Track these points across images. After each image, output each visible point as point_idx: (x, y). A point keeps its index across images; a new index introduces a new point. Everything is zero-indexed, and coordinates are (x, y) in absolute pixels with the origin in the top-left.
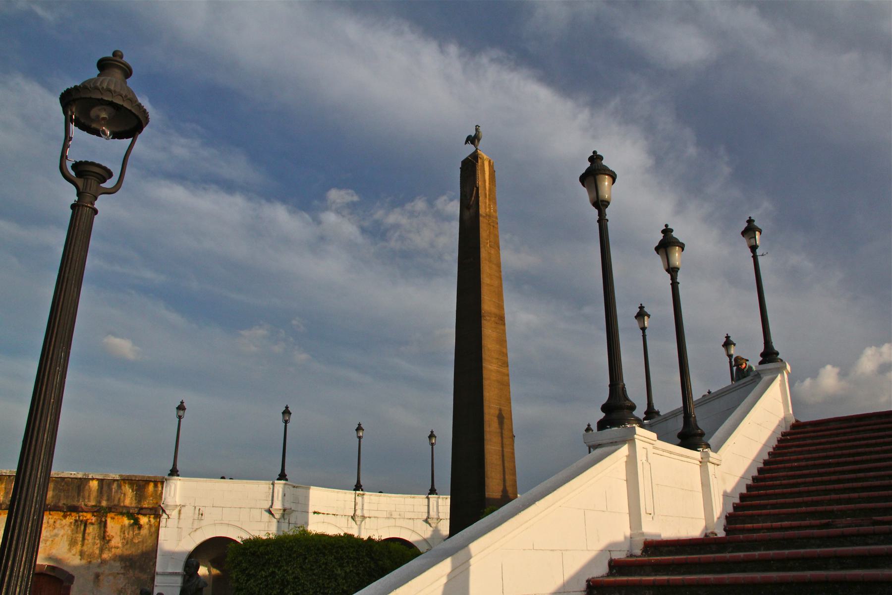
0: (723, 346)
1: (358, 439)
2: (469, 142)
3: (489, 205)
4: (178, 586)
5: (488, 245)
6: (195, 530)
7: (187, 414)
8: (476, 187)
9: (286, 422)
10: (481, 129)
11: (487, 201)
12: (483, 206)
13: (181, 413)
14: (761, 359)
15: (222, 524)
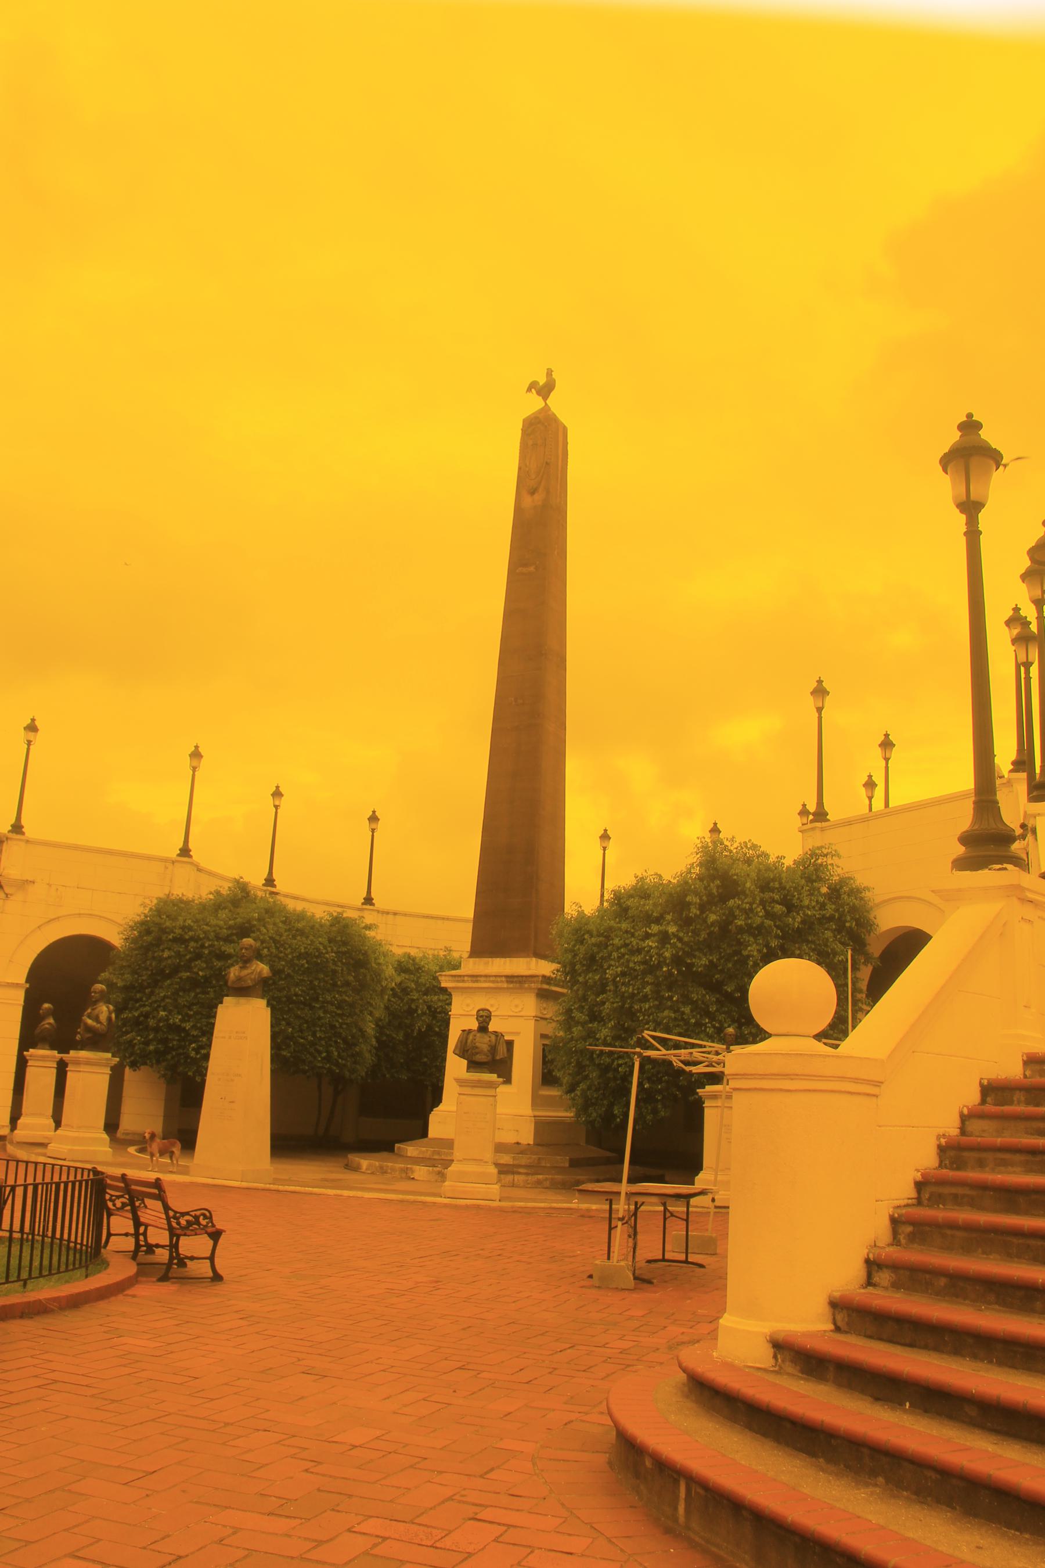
0: (880, 745)
2: (533, 390)
4: (19, 1005)
5: (556, 553)
6: (49, 921)
7: (39, 739)
8: (547, 463)
10: (554, 376)
11: (559, 487)
13: (31, 736)
15: (90, 915)
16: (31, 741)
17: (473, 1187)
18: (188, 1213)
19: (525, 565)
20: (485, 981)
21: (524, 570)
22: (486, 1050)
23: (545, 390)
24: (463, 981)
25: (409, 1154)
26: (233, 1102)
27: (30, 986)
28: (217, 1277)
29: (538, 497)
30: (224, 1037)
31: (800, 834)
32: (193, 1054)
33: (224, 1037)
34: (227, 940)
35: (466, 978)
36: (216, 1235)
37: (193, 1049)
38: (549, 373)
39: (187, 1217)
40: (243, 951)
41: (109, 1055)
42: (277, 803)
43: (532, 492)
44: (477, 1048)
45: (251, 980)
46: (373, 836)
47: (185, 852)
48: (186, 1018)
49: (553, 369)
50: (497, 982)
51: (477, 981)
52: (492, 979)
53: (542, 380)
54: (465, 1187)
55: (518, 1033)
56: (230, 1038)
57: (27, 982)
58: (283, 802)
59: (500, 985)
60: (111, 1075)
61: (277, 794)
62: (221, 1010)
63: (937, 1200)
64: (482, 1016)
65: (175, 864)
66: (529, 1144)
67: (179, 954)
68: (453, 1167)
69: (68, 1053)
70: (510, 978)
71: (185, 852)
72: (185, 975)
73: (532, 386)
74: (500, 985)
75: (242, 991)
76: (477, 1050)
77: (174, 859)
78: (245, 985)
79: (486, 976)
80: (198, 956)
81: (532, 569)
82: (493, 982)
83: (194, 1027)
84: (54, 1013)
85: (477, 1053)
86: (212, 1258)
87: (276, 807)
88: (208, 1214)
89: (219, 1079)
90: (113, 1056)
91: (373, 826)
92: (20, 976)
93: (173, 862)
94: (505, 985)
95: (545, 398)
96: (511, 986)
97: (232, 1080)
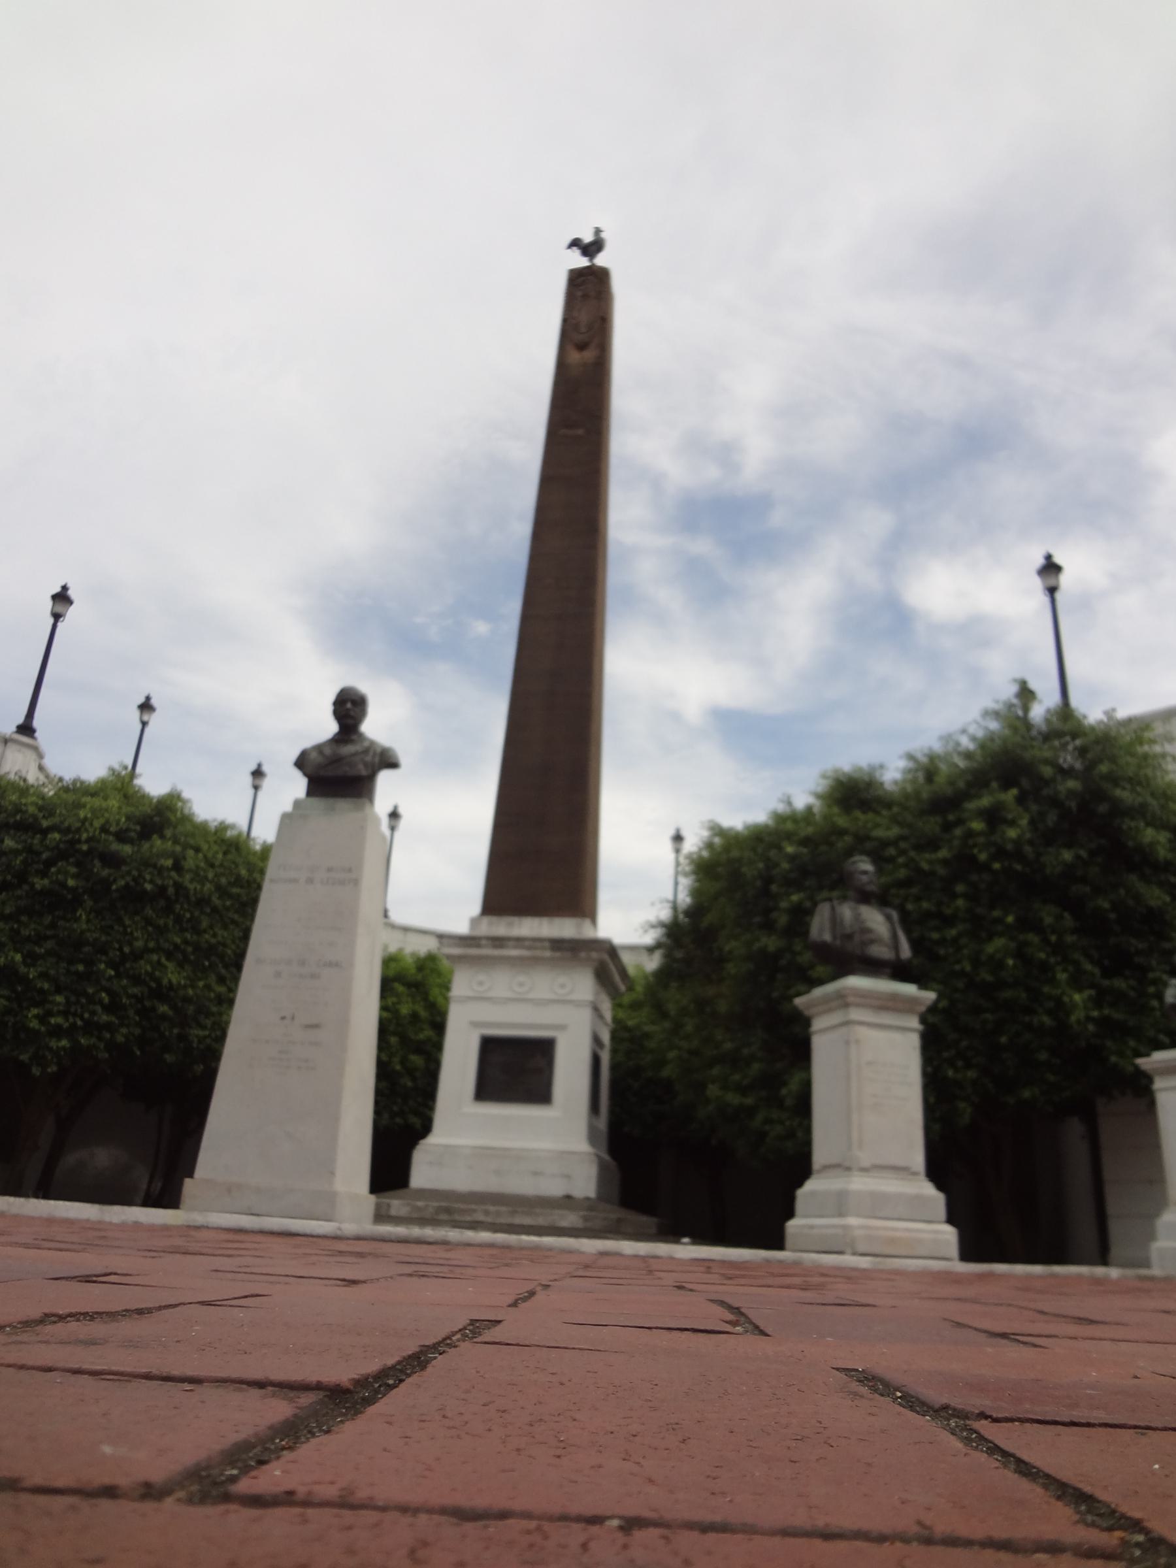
9: (57, 617)
10: (603, 235)
17: (907, 1230)
20: (515, 947)
23: (592, 248)
24: (479, 946)
25: (393, 1212)
26: (316, 1026)
29: (589, 355)
30: (295, 881)
32: (34, 1024)
33: (295, 881)
34: (121, 836)
35: (484, 942)
37: (36, 1017)
38: (598, 231)
40: (349, 705)
42: (145, 718)
43: (581, 347)
44: (868, 931)
45: (366, 765)
47: (26, 729)
48: (31, 959)
49: (602, 229)
50: (536, 948)
51: (501, 946)
52: (527, 943)
53: (588, 238)
55: (562, 1027)
58: (154, 719)
59: (538, 953)
61: (146, 706)
65: (9, 744)
66: (588, 1199)
67: (29, 850)
70: (557, 944)
71: (26, 729)
72: (40, 883)
73: (575, 243)
74: (538, 953)
77: (7, 736)
79: (519, 941)
80: (62, 854)
81: (580, 432)
82: (529, 948)
83: (44, 976)
85: (872, 942)
87: (144, 724)
91: (257, 782)
93: (6, 741)
94: (548, 954)
95: (591, 260)
96: (558, 954)
97: (314, 976)
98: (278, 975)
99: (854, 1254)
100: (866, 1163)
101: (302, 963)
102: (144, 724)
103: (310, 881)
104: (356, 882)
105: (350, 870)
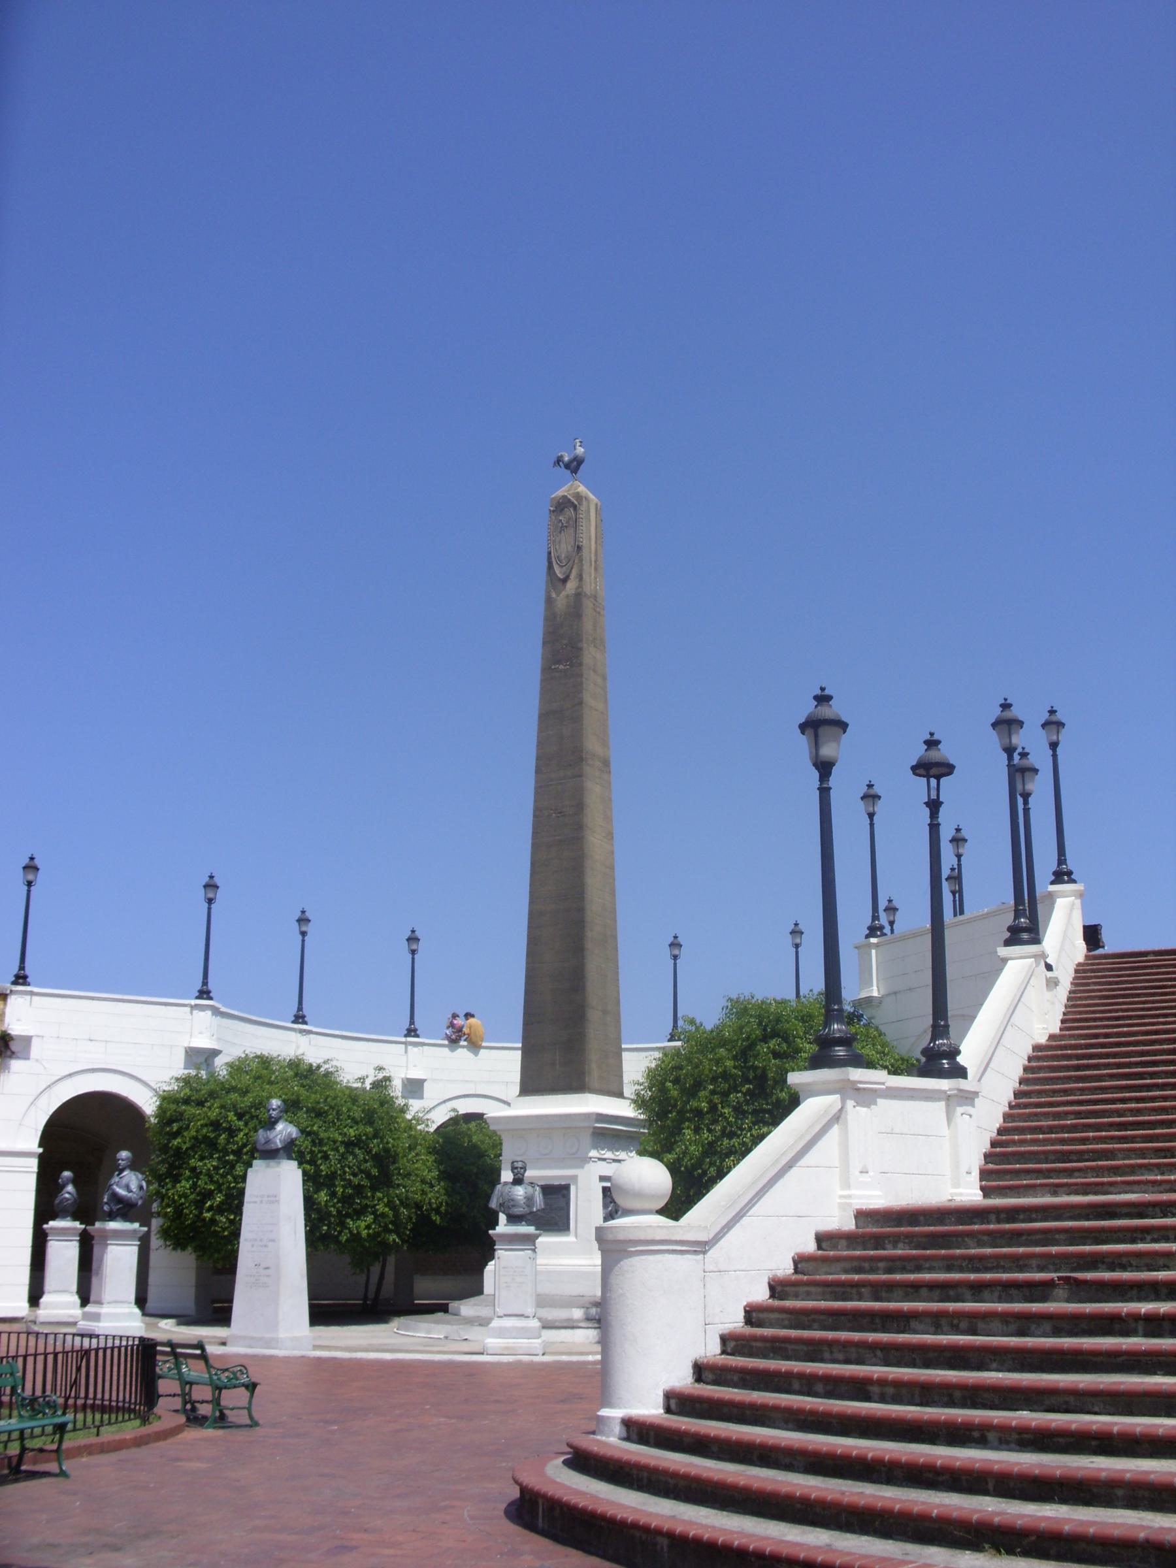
1: (300, 937)
3: (596, 578)
12: (588, 580)
14: (1053, 878)
16: (32, 882)
18: (227, 1370)
19: (559, 662)
21: (561, 667)
22: (522, 1202)
27: (44, 1151)
28: (254, 1424)
29: (571, 586)
30: (256, 1202)
31: (856, 951)
33: (256, 1202)
36: (252, 1387)
39: (226, 1374)
41: (136, 1225)
42: (304, 929)
44: (513, 1200)
46: (413, 959)
54: (508, 1343)
56: (261, 1202)
57: (40, 1146)
60: (139, 1246)
62: (251, 1174)
63: (760, 1324)
64: (517, 1168)
68: (496, 1323)
69: (94, 1225)
75: (271, 1154)
76: (512, 1203)
78: (273, 1147)
84: (75, 1182)
85: (513, 1206)
86: (249, 1409)
87: (304, 934)
88: (243, 1368)
89: (253, 1246)
90: (141, 1226)
92: (32, 1143)
97: (266, 1246)
98: (253, 1246)
99: (487, 1354)
100: (500, 1314)
101: (261, 1240)
102: (304, 934)
103: (261, 1202)
104: (278, 1201)
105: (276, 1197)
